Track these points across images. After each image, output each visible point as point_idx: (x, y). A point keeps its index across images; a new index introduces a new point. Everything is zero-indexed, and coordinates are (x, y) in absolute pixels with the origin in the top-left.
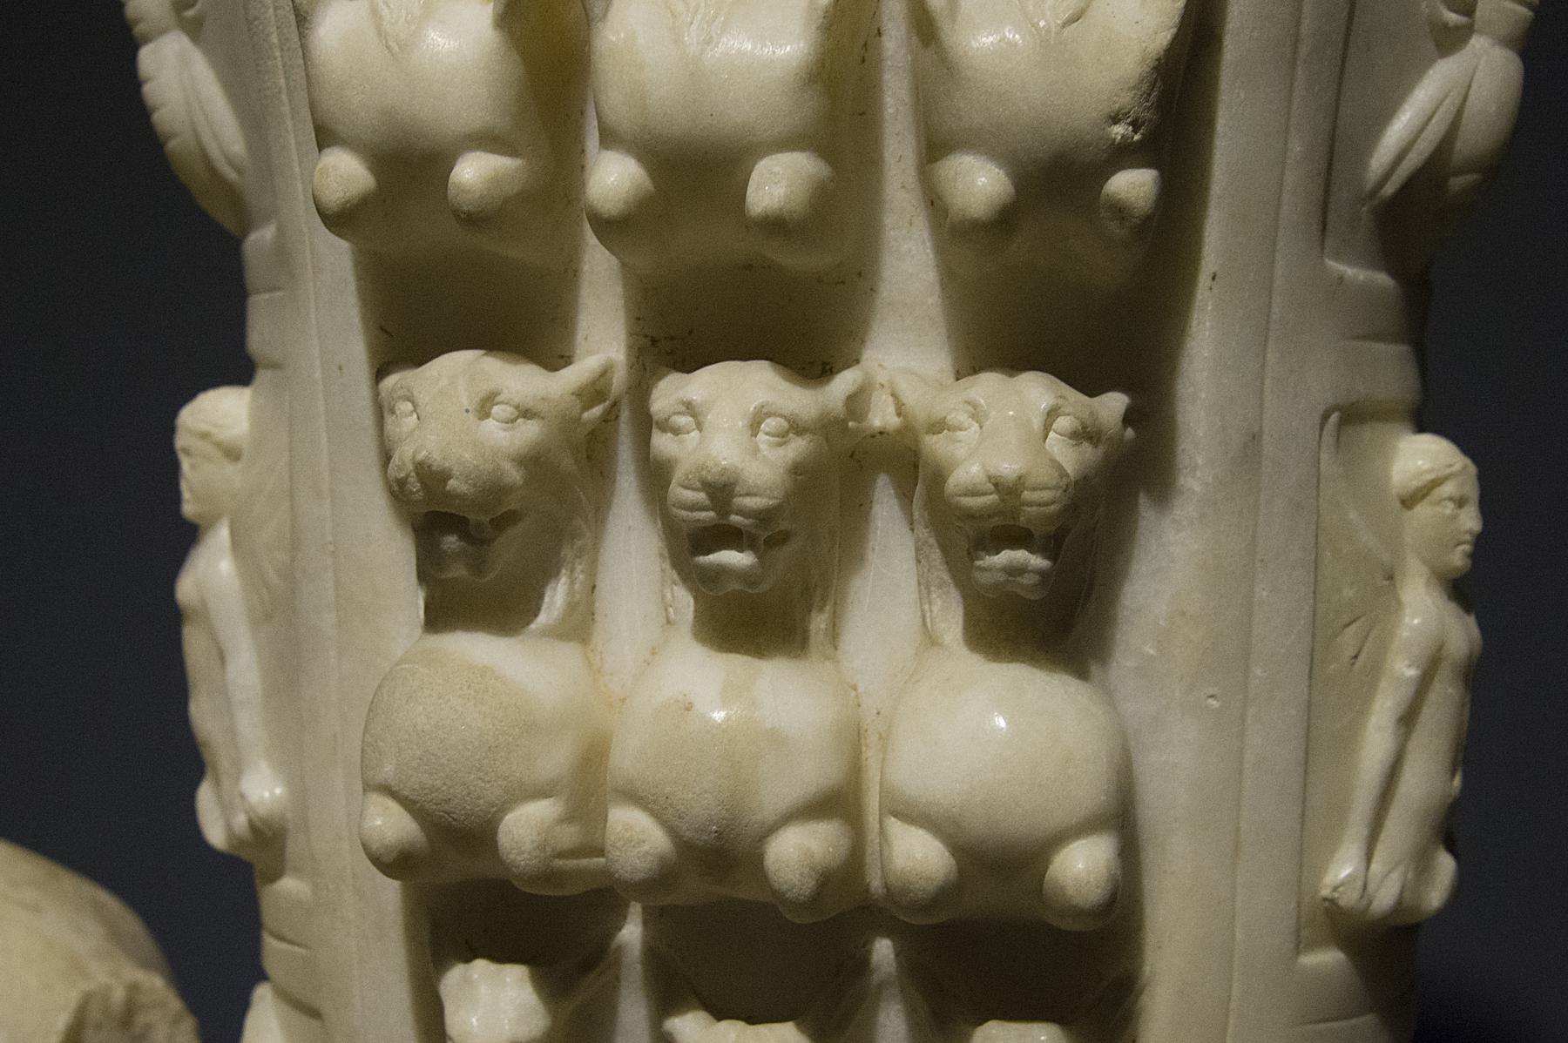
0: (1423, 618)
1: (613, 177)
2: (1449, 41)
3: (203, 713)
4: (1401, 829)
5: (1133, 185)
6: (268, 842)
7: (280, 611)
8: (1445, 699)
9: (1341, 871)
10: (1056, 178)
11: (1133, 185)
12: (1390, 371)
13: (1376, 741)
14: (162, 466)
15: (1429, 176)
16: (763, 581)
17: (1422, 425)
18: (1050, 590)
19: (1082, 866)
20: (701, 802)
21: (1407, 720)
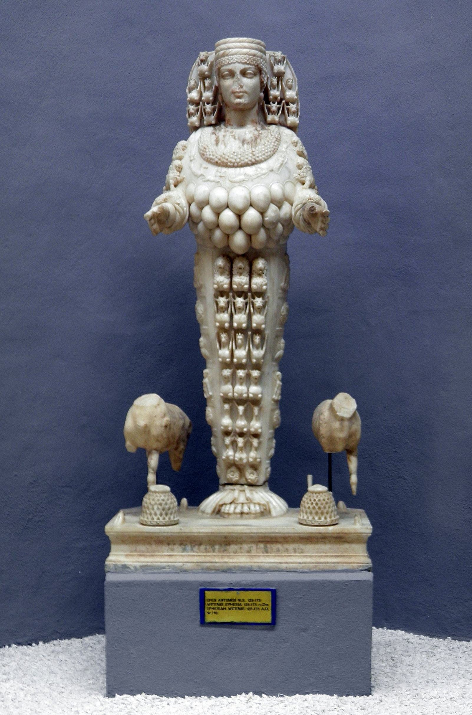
0: (279, 383)
1: (235, 360)
2: (279, 350)
3: (205, 389)
4: (277, 395)
5: (262, 361)
6: (211, 397)
7: (212, 383)
8: (280, 388)
9: (274, 396)
10: (258, 359)
11: (262, 361)
12: (276, 368)
13: (276, 389)
14: (202, 373)
15: (278, 358)
16: (242, 381)
17: (280, 371)
18: (258, 381)
19: (260, 396)
20: (240, 392)
21: (278, 389)
